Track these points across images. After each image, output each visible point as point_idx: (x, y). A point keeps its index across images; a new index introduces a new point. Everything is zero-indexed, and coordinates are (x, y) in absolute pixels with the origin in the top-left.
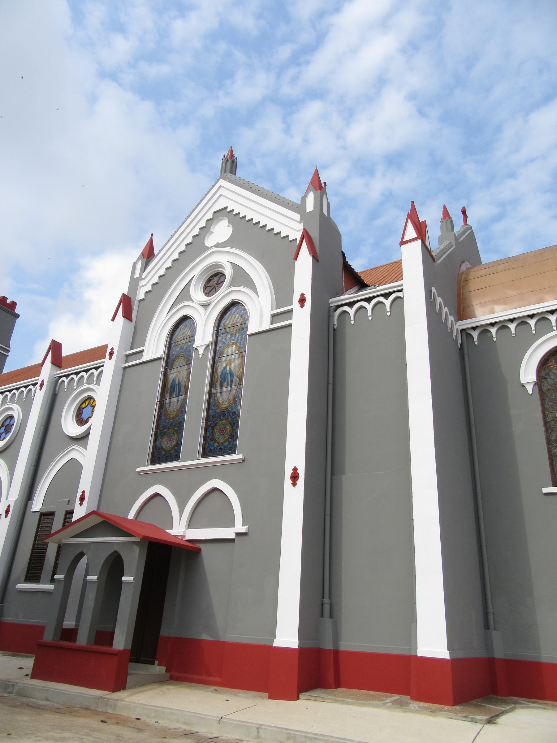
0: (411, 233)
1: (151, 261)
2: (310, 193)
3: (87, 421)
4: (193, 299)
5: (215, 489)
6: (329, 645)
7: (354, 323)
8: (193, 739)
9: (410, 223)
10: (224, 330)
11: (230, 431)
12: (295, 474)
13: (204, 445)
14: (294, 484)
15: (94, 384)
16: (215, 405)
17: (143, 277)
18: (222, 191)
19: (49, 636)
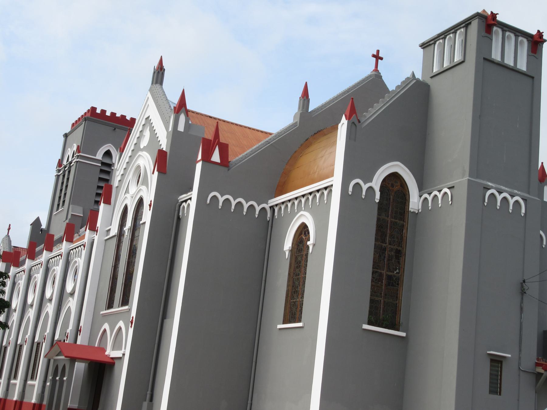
17: (118, 169)
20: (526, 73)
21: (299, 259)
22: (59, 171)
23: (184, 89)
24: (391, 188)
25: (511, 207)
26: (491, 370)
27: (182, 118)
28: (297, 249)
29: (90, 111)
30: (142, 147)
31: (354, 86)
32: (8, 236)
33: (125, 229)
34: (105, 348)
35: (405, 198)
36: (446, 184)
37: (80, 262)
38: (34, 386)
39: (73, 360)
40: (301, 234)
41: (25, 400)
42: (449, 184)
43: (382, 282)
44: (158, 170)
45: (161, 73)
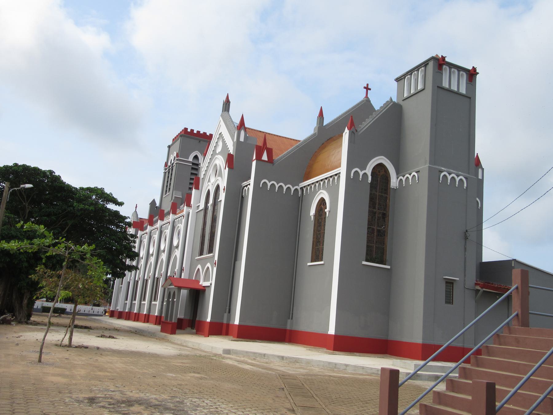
6: (225, 322)
20: (465, 95)
21: (320, 221)
22: (166, 169)
23: (243, 114)
24: (378, 173)
25: (457, 183)
26: (446, 288)
27: (243, 133)
28: (319, 214)
29: (184, 131)
30: (217, 152)
31: (353, 108)
32: (136, 211)
33: (208, 205)
34: (199, 280)
35: (388, 180)
36: (414, 170)
37: (181, 226)
38: (156, 305)
39: (180, 288)
40: (321, 205)
41: (151, 314)
42: (416, 169)
43: (374, 234)
44: (228, 167)
45: (228, 104)
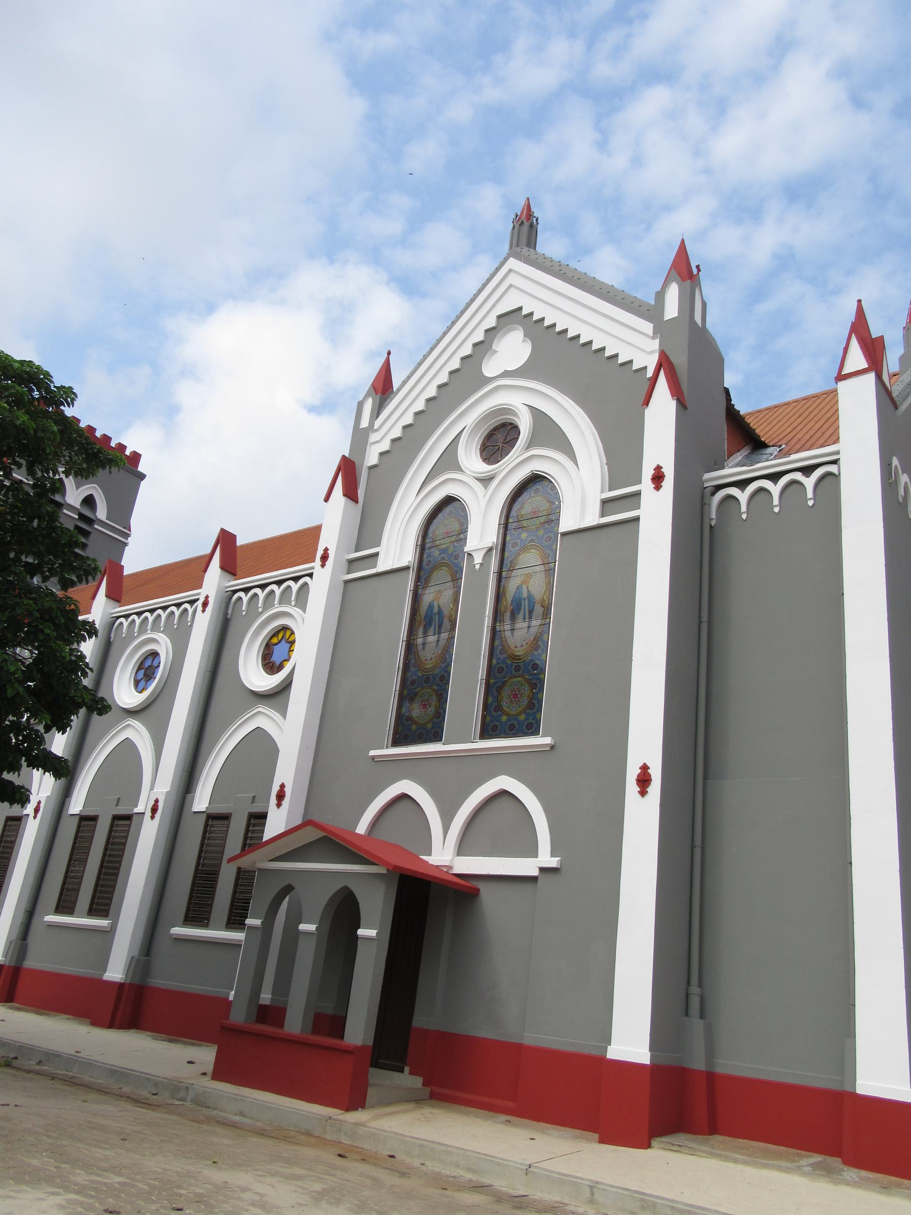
0: (857, 359)
1: (389, 400)
2: (671, 284)
3: (280, 667)
4: (463, 468)
5: (503, 793)
6: (698, 1064)
7: (747, 518)
8: (490, 1196)
9: (855, 344)
10: (517, 524)
11: (528, 697)
12: (644, 775)
13: (484, 717)
14: (643, 793)
15: (292, 606)
16: (503, 651)
17: (376, 427)
18: (512, 279)
19: (239, 1016)
